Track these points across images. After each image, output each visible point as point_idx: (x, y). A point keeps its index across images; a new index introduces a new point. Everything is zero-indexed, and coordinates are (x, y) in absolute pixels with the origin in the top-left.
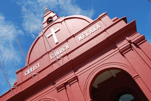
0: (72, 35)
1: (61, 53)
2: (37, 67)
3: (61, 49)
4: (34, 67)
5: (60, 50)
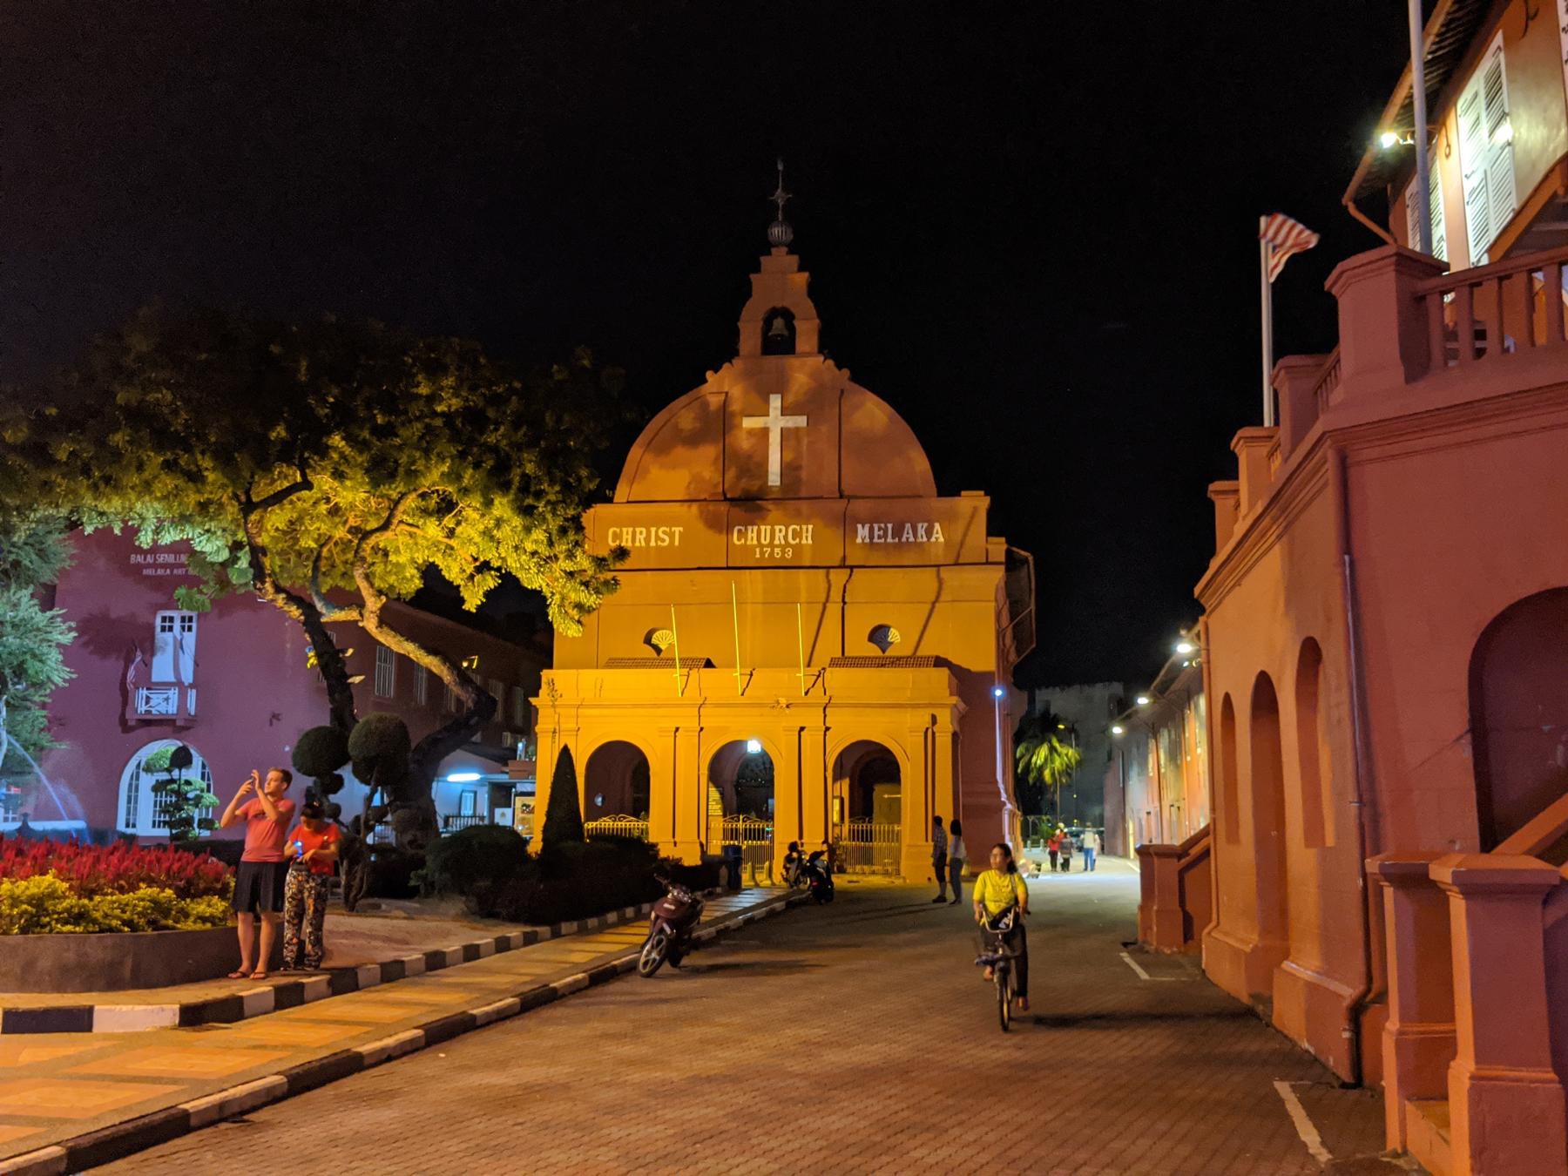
1: (777, 546)
3: (783, 528)
4: (657, 532)
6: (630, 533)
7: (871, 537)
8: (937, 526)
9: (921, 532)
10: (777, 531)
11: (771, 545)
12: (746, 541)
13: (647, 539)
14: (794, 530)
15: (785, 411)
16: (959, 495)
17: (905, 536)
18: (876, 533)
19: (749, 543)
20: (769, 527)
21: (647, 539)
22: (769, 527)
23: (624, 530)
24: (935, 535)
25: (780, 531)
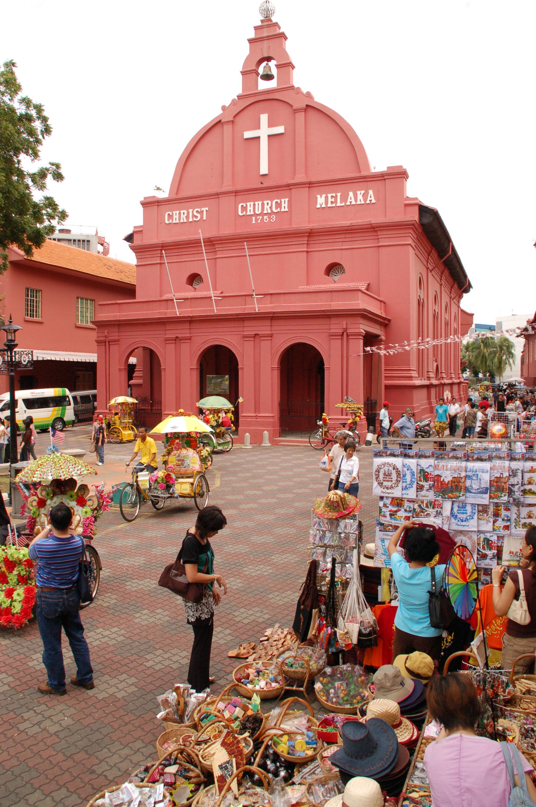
0: (308, 180)
1: (266, 214)
2: (199, 215)
3: (269, 202)
4: (193, 212)
5: (265, 202)
6: (178, 214)
7: (326, 203)
8: (371, 192)
9: (360, 197)
10: (266, 204)
11: (262, 214)
12: (246, 212)
13: (188, 217)
14: (277, 202)
15: (270, 125)
16: (388, 168)
17: (349, 200)
18: (330, 200)
19: (248, 213)
20: (260, 203)
21: (188, 217)
22: (260, 203)
23: (174, 213)
24: (369, 199)
25: (268, 203)
